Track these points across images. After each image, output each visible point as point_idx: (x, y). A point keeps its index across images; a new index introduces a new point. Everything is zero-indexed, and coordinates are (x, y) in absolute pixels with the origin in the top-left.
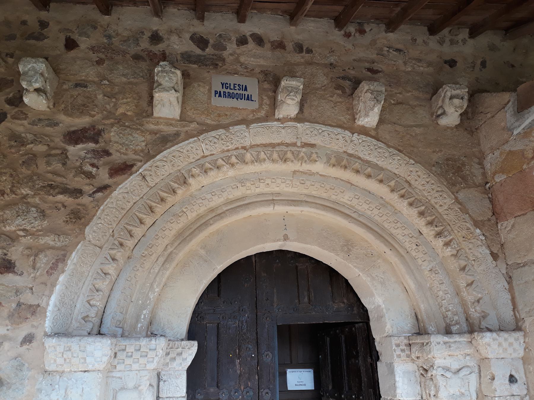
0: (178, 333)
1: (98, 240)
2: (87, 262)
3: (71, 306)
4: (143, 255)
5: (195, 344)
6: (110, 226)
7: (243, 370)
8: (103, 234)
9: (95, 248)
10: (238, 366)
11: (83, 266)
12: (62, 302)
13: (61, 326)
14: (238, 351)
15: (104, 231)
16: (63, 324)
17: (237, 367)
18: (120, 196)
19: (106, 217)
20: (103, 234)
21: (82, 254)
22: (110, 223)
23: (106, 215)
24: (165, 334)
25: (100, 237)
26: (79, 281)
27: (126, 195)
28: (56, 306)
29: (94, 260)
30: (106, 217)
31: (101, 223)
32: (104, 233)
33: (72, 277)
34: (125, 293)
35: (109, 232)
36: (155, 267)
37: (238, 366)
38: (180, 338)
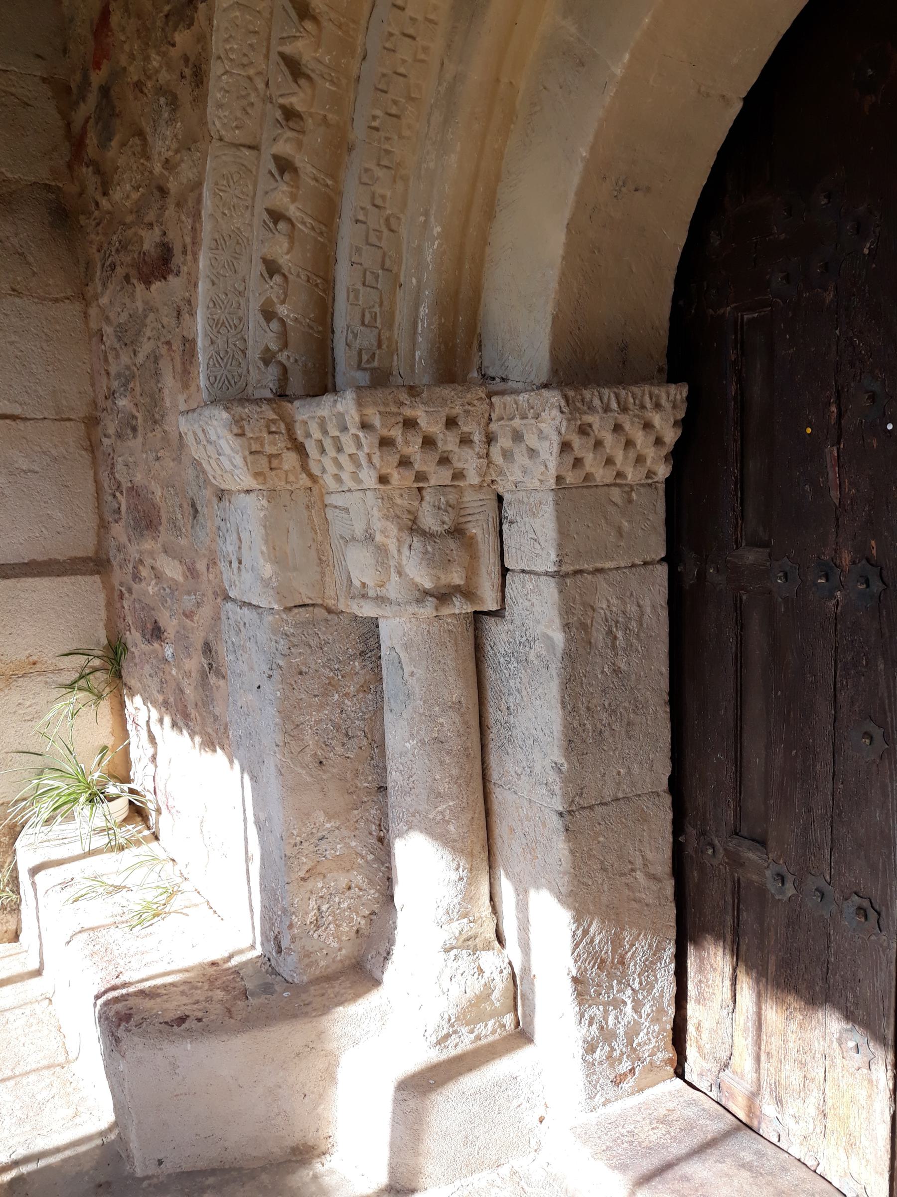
0: (531, 366)
1: (237, 127)
2: (235, 200)
3: (236, 327)
4: (374, 124)
5: (679, 392)
6: (251, 72)
7: (850, 490)
8: (244, 102)
9: (238, 153)
10: (833, 474)
11: (231, 216)
12: (215, 324)
13: (226, 382)
14: (834, 409)
15: (243, 93)
16: (230, 377)
17: (831, 475)
19: (228, 47)
20: (244, 102)
21: (216, 184)
22: (245, 61)
23: (227, 41)
24: (506, 373)
25: (239, 114)
26: (236, 258)
28: (206, 335)
29: (251, 187)
30: (228, 47)
31: (226, 72)
32: (244, 97)
33: (216, 252)
34: (361, 264)
35: (256, 89)
36: (428, 153)
37: (833, 474)
38: (537, 382)
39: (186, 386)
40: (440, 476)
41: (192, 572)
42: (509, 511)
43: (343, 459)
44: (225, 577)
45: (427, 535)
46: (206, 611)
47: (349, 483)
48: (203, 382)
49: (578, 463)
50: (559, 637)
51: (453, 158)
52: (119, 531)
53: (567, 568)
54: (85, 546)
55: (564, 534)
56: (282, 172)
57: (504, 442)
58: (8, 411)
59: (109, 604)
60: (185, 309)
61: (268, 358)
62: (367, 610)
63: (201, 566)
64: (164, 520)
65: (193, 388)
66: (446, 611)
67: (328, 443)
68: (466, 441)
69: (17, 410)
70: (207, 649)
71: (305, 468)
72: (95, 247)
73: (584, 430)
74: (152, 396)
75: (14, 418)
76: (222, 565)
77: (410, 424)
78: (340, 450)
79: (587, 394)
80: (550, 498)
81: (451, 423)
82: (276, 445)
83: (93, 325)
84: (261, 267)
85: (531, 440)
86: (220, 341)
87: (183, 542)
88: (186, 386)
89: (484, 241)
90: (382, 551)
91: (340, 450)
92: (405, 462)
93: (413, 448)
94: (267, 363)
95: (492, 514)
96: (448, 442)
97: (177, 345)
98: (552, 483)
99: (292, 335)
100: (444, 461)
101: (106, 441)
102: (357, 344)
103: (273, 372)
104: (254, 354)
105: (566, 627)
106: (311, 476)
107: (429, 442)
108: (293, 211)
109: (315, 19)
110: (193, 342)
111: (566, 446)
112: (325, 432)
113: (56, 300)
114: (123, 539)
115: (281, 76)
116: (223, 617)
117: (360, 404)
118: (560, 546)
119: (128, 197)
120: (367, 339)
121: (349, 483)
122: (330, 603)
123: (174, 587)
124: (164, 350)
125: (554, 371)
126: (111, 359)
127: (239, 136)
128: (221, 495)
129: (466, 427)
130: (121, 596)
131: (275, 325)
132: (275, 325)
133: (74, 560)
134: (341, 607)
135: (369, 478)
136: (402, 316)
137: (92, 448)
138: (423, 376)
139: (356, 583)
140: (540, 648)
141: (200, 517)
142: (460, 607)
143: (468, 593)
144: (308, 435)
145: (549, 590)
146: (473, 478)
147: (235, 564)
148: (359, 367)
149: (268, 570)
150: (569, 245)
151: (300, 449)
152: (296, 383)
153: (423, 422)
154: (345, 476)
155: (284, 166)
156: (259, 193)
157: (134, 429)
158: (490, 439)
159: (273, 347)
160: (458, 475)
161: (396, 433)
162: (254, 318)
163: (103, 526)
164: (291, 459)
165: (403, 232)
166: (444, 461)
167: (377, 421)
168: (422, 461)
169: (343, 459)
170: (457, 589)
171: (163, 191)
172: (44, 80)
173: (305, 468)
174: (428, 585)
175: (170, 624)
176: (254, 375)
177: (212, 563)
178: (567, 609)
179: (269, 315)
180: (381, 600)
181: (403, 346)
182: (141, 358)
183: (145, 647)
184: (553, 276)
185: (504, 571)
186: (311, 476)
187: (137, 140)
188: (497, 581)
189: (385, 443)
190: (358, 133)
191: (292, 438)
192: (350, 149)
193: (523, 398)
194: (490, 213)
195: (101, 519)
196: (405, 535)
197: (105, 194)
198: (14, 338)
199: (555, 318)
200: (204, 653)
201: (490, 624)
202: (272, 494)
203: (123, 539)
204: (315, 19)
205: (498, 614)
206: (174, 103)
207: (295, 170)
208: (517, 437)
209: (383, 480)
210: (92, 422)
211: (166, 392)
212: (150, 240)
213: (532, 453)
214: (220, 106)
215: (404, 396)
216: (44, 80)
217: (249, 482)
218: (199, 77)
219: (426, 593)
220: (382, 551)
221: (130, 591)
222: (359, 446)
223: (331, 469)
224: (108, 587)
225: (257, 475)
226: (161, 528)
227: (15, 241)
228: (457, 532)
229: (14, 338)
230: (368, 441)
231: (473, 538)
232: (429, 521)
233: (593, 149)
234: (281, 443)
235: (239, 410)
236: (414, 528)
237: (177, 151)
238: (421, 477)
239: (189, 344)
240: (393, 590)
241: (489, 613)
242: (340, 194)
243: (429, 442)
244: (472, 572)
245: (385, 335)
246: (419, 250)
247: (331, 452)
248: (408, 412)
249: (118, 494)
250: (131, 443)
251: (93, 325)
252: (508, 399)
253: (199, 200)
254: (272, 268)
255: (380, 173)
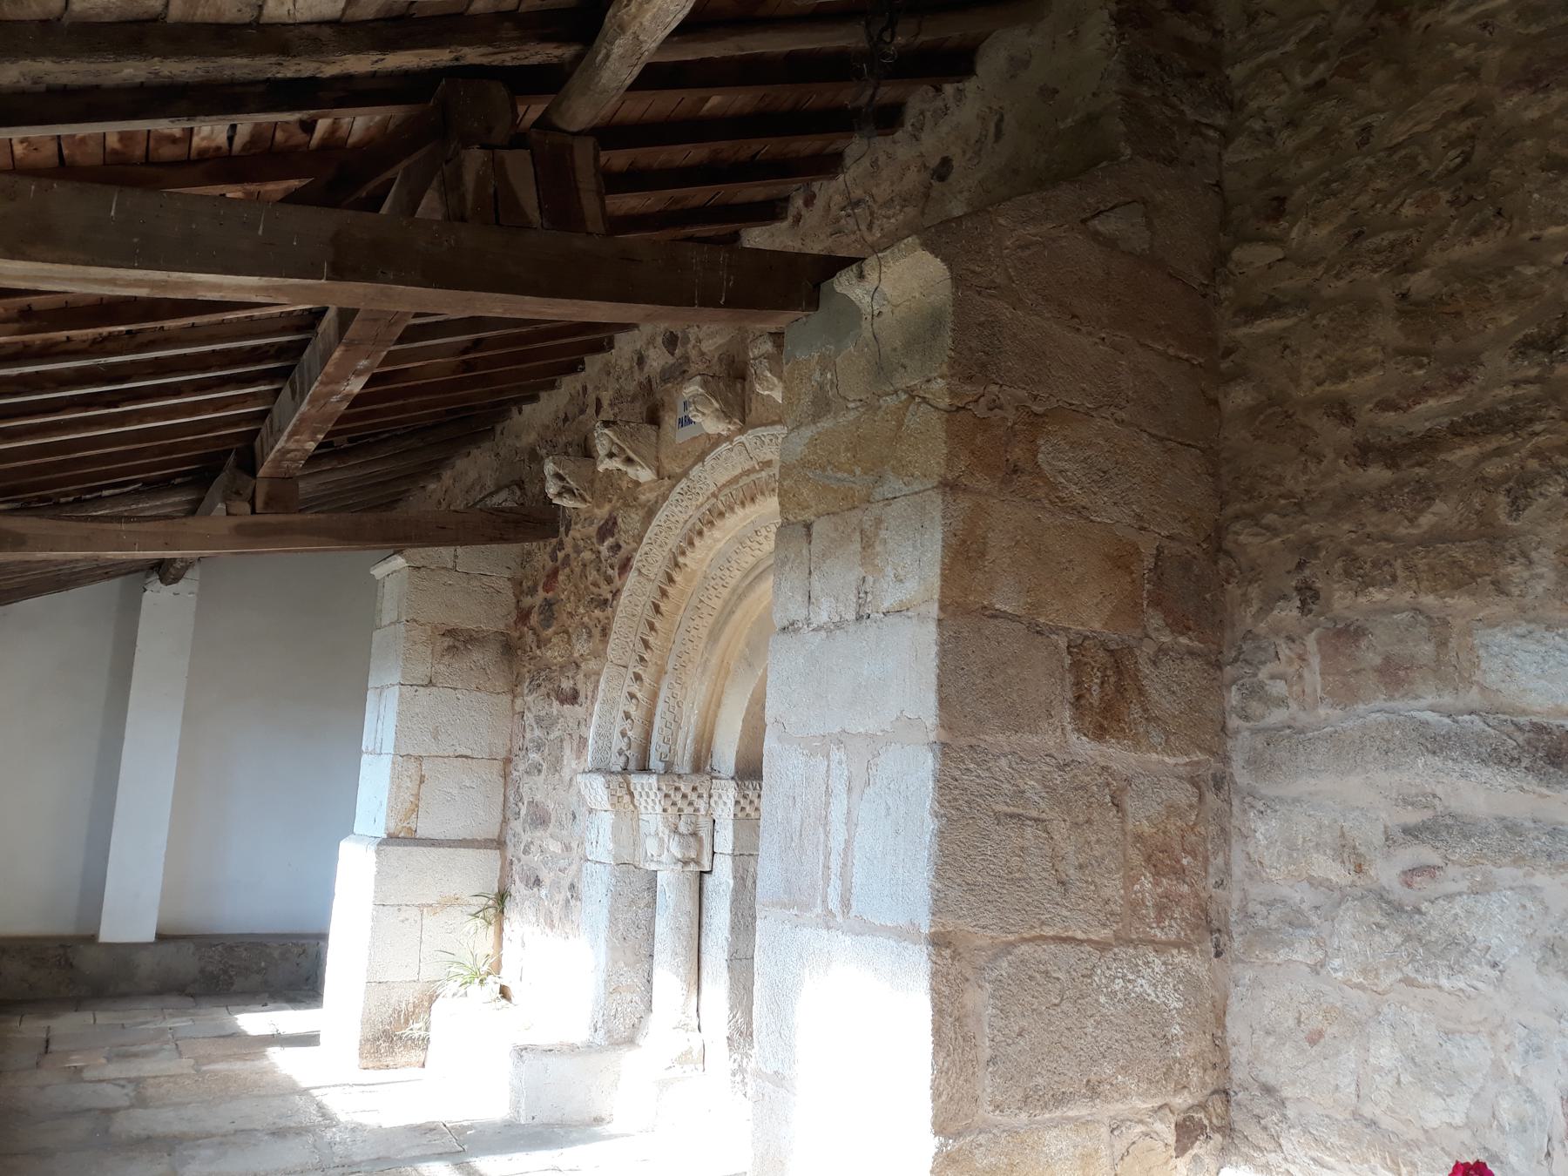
12: (598, 734)
18: (626, 601)
27: (630, 598)
39: (578, 758)
40: (688, 810)
41: (568, 848)
42: (717, 827)
43: (649, 801)
44: (587, 851)
45: (681, 835)
46: (574, 867)
47: (650, 810)
48: (589, 758)
49: (743, 809)
50: (731, 882)
51: (704, 688)
52: (516, 825)
53: (737, 853)
54: (493, 833)
55: (736, 837)
56: (636, 680)
57: (715, 798)
58: (464, 753)
59: (502, 868)
60: (583, 723)
61: (620, 753)
62: (653, 867)
63: (574, 845)
64: (553, 820)
65: (582, 759)
66: (687, 869)
67: (644, 793)
68: (700, 796)
69: (469, 753)
70: (572, 887)
71: (632, 802)
72: (526, 670)
73: (745, 797)
74: (557, 758)
75: (466, 757)
76: (587, 845)
77: (677, 789)
78: (648, 797)
79: (747, 783)
80: (731, 822)
81: (694, 789)
82: (622, 792)
83: (517, 709)
84: (623, 715)
85: (724, 798)
86: (600, 743)
87: (564, 832)
88: (578, 758)
89: (716, 716)
90: (661, 840)
91: (648, 797)
92: (674, 804)
93: (678, 798)
94: (620, 755)
95: (710, 827)
96: (693, 796)
97: (576, 737)
98: (732, 816)
99: (633, 745)
100: (691, 804)
101: (515, 773)
102: (660, 750)
103: (622, 760)
104: (615, 749)
105: (735, 877)
106: (634, 805)
107: (684, 796)
108: (639, 695)
109: (656, 631)
110: (586, 740)
111: (737, 803)
112: (643, 789)
113: (499, 693)
114: (519, 829)
115: (640, 647)
116: (584, 869)
117: (658, 781)
118: (734, 843)
119: (555, 658)
120: (665, 749)
121: (650, 810)
122: (637, 864)
123: (554, 856)
124: (567, 737)
125: (737, 772)
126: (527, 730)
127: (619, 662)
128: (591, 811)
129: (700, 791)
130: (511, 863)
131: (626, 739)
132: (626, 739)
133: (486, 840)
134: (641, 866)
135: (659, 809)
136: (680, 742)
137: (505, 776)
138: (687, 769)
139: (649, 854)
140: (724, 887)
141: (577, 820)
142: (693, 867)
143: (697, 863)
144: (636, 789)
145: (729, 860)
146: (703, 812)
147: (594, 843)
148: (660, 760)
149: (611, 846)
150: (743, 726)
151: (631, 794)
152: (632, 766)
153: (683, 788)
154: (649, 807)
155: (638, 677)
156: (626, 685)
157: (540, 771)
158: (710, 796)
159: (624, 748)
160: (696, 810)
161: (672, 793)
162: (616, 735)
163: (505, 821)
164: (627, 798)
165: (684, 707)
166: (691, 804)
167: (664, 788)
168: (680, 803)
169: (649, 801)
170: (693, 860)
171: (578, 666)
172: (509, 579)
173: (632, 802)
174: (679, 856)
175: (547, 877)
176: (613, 759)
177: (582, 843)
178: (735, 870)
179: (623, 734)
180: (659, 862)
181: (680, 754)
182: (552, 737)
183: (525, 892)
184: (738, 736)
185: (714, 853)
186: (634, 805)
187: (566, 636)
188: (710, 858)
189: (666, 796)
190: (669, 667)
191: (629, 789)
192: (666, 673)
193: (723, 782)
194: (718, 706)
195: (504, 817)
196: (672, 834)
197: (539, 647)
198: (473, 713)
199: (737, 752)
200: (570, 889)
201: (707, 878)
202: (617, 813)
203: (519, 829)
204: (656, 631)
205: (709, 872)
206: (590, 635)
207: (642, 680)
208: (720, 796)
209: (665, 810)
210: (508, 761)
211: (565, 757)
212: (566, 685)
213: (725, 803)
214: (613, 650)
215: (676, 778)
216: (509, 579)
217: (608, 807)
218: (605, 632)
219: (679, 860)
220: (661, 840)
221: (519, 860)
222: (656, 796)
223: (644, 804)
224: (503, 857)
225: (612, 804)
226: (551, 826)
227: (482, 662)
228: (694, 834)
229: (473, 713)
230: (660, 795)
231: (701, 838)
232: (683, 829)
233: (752, 695)
234: (624, 791)
235: (608, 778)
236: (676, 831)
237: (588, 654)
238: (680, 810)
239: (583, 741)
240: (664, 858)
241: (706, 872)
242: (659, 689)
243: (684, 796)
244: (700, 853)
245: (673, 747)
246: (689, 717)
247: (644, 797)
248: (677, 784)
249: (520, 804)
250: (536, 778)
251: (517, 709)
252: (718, 781)
253: (598, 681)
254: (627, 716)
255: (677, 685)
